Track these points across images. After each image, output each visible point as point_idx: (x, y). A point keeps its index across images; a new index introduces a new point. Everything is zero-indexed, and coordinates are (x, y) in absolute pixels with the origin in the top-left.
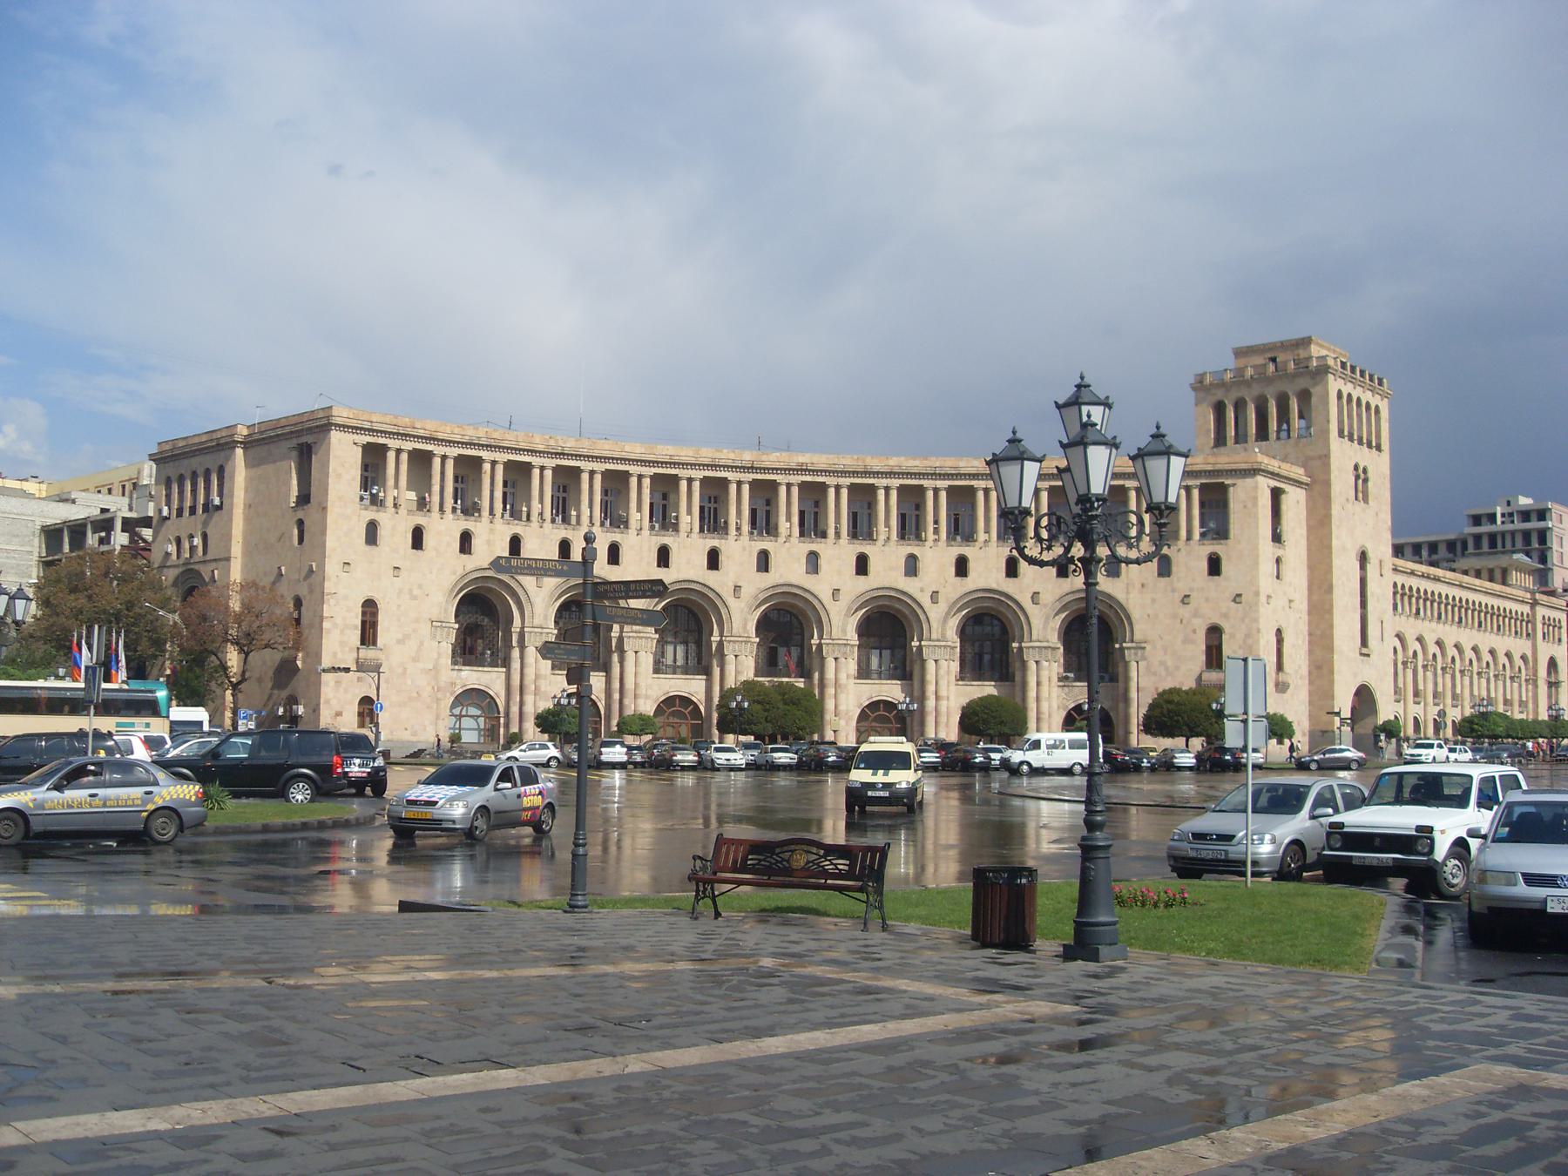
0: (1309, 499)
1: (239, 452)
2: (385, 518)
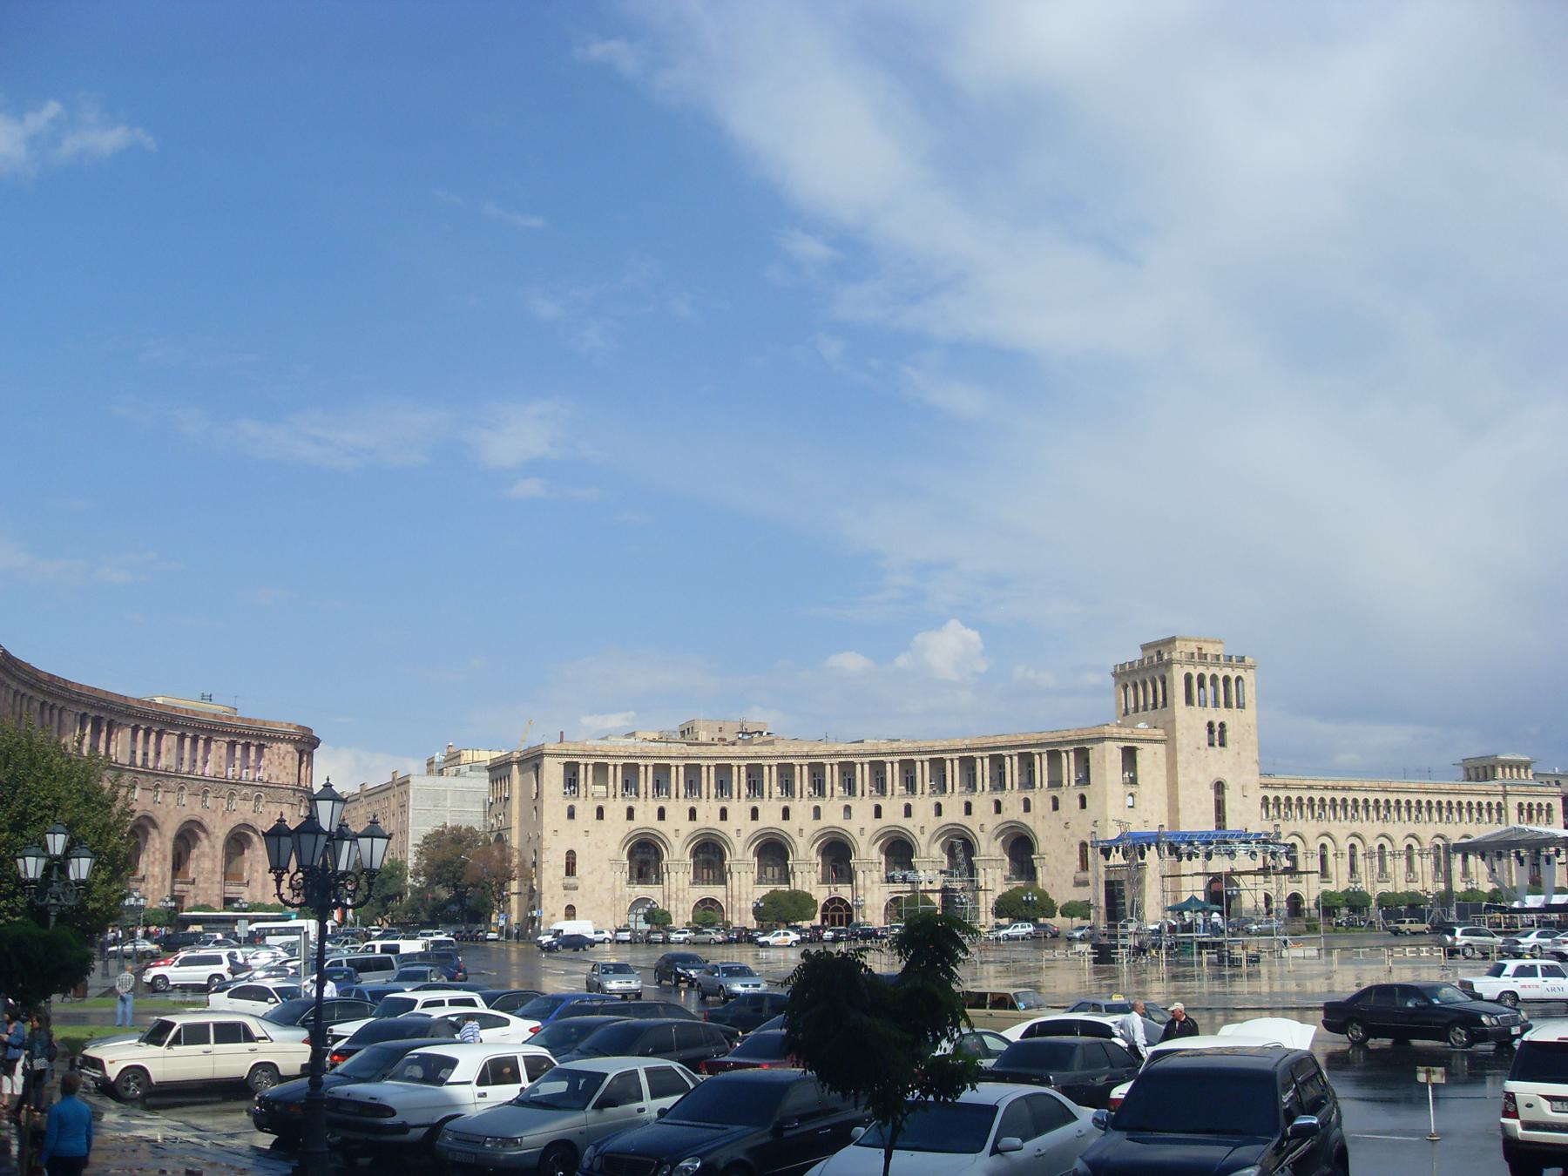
1: (515, 767)
2: (579, 805)
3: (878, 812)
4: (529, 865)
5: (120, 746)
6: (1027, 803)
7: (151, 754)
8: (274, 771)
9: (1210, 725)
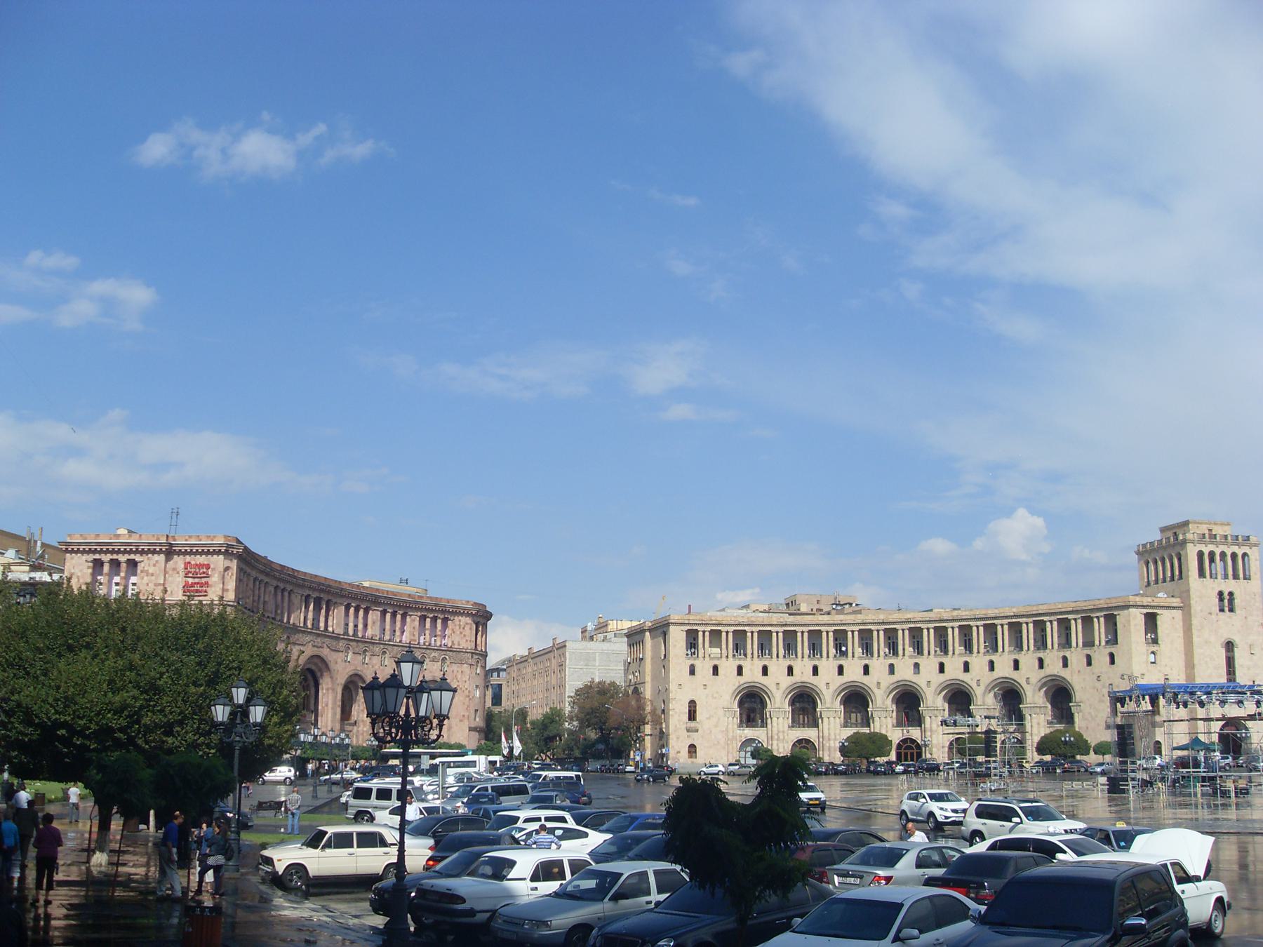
0: (1183, 615)
1: (647, 634)
2: (698, 663)
3: (942, 668)
4: (659, 712)
5: (336, 620)
6: (1065, 660)
7: (360, 626)
8: (456, 639)
9: (1221, 594)
